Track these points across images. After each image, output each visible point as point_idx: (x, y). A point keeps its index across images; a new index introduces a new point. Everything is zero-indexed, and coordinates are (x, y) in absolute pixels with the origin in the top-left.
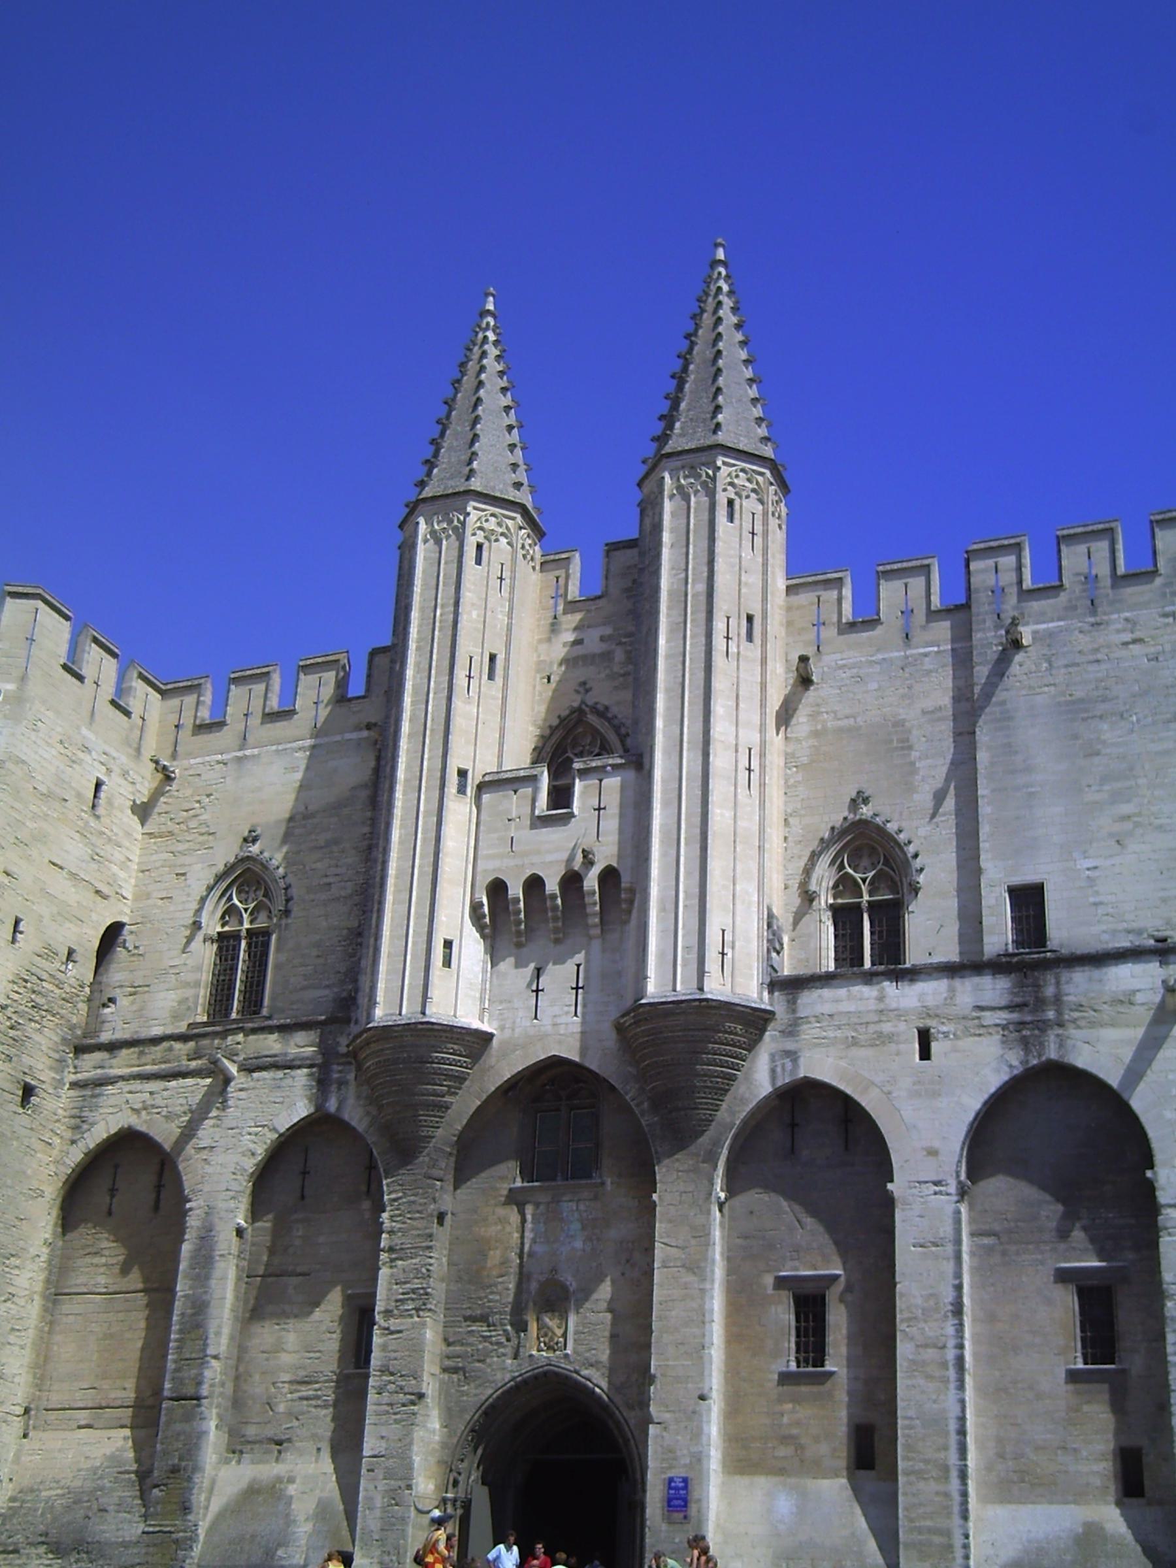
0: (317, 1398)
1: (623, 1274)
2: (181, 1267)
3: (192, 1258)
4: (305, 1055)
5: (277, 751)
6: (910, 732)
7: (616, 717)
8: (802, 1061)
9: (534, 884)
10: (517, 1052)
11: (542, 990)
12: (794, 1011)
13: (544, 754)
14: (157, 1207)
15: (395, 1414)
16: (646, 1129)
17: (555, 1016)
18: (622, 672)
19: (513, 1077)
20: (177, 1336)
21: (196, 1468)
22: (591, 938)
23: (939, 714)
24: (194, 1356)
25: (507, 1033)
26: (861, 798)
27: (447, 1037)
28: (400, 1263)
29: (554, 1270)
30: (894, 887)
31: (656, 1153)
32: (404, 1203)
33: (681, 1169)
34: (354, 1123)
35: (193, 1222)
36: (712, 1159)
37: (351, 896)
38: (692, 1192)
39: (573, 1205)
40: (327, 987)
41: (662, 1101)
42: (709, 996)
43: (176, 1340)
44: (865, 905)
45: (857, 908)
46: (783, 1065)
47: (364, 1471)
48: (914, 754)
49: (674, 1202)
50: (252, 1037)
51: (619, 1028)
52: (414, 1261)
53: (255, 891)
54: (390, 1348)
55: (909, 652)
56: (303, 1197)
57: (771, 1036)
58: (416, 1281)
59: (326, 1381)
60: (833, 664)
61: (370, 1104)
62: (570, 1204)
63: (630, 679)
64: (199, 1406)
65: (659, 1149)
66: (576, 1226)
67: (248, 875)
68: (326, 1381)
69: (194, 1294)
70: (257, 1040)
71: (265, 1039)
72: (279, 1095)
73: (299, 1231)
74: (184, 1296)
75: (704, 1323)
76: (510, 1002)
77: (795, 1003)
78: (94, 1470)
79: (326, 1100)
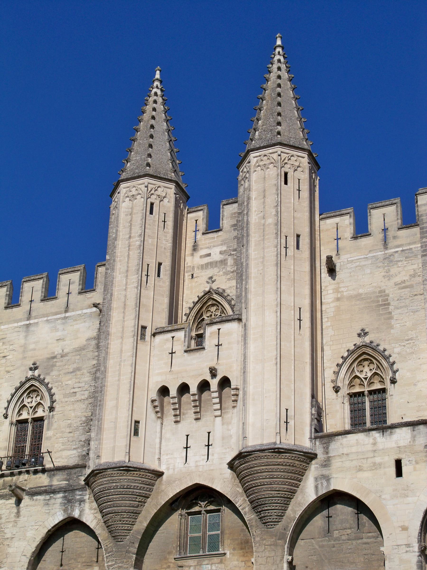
4: (62, 486)
5: (47, 320)
6: (388, 296)
7: (229, 295)
8: (332, 481)
10: (176, 482)
12: (327, 453)
18: (232, 270)
23: (404, 285)
25: (171, 472)
26: (363, 333)
27: (137, 474)
30: (382, 382)
32: (116, 567)
33: (267, 544)
34: (88, 523)
38: (273, 557)
39: (209, 566)
40: (74, 449)
42: (280, 446)
44: (366, 393)
45: (361, 394)
46: (322, 483)
48: (391, 308)
49: (263, 563)
51: (231, 465)
53: (36, 397)
55: (386, 252)
56: (61, 565)
57: (315, 467)
60: (346, 260)
61: (97, 513)
62: (208, 566)
65: (255, 533)
67: (32, 389)
70: (36, 478)
71: (40, 478)
72: (47, 509)
76: (172, 454)
77: (328, 448)
79: (73, 510)
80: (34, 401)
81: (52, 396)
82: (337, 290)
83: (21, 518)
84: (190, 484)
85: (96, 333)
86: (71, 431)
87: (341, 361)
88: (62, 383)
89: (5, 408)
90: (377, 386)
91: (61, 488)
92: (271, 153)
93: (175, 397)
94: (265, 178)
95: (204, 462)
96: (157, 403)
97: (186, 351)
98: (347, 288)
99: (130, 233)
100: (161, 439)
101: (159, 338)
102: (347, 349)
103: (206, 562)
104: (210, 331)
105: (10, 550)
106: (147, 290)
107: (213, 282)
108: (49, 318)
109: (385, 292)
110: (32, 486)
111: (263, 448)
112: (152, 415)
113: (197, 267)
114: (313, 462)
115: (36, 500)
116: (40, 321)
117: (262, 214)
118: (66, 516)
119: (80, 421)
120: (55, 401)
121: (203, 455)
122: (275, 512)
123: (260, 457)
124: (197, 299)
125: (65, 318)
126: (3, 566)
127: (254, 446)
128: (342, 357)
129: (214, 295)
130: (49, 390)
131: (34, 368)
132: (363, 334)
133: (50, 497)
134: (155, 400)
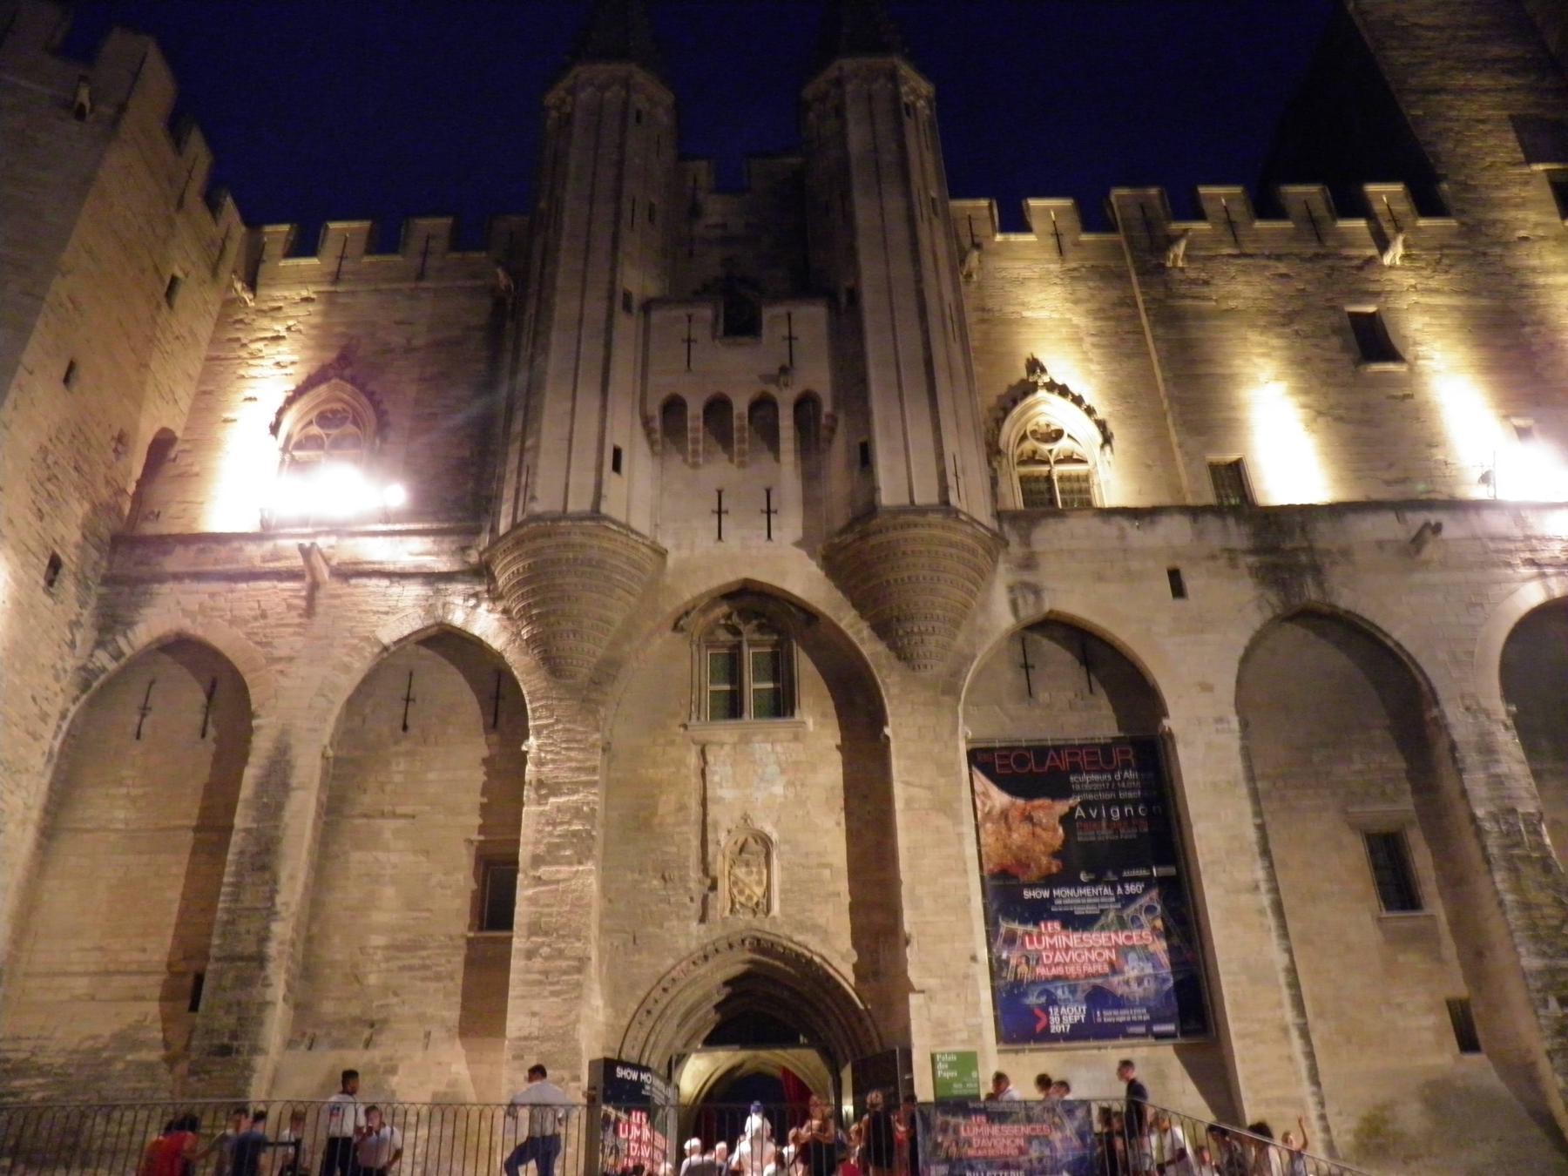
0: (425, 967)
15: (552, 984)
20: (231, 880)
21: (256, 1049)
25: (685, 553)
29: (745, 818)
35: (262, 745)
36: (951, 689)
43: (232, 884)
54: (542, 902)
56: (405, 728)
59: (440, 947)
64: (262, 967)
66: (773, 769)
68: (440, 947)
69: (257, 829)
73: (400, 765)
74: (248, 831)
75: (965, 871)
78: (97, 1051)
101: (656, 317)
103: (759, 737)
104: (771, 314)
105: (284, 682)
115: (356, 586)
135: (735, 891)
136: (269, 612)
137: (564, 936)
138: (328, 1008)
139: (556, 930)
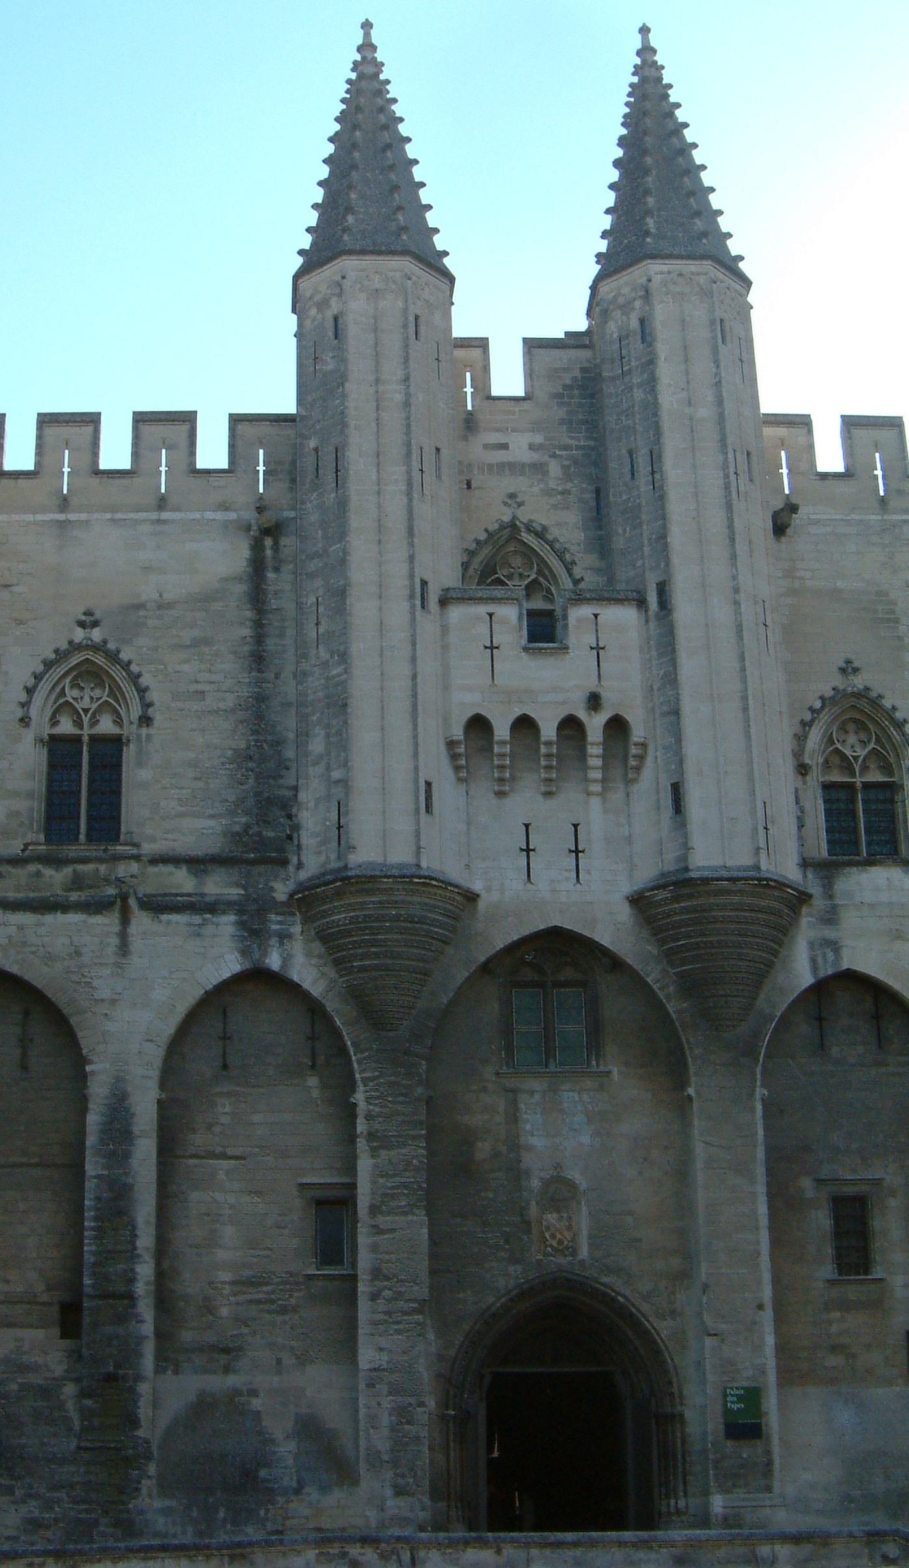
0: (273, 1302)
1: (640, 1173)
2: (88, 1143)
3: (102, 1131)
5: (112, 520)
8: (845, 953)
9: (525, 725)
11: (533, 850)
12: (831, 897)
13: (471, 571)
14: (25, 1067)
15: (398, 1323)
16: (674, 1016)
17: (553, 881)
18: (560, 489)
19: (506, 946)
21: (138, 1378)
22: (589, 794)
24: (119, 1247)
25: (495, 896)
26: (848, 669)
28: (383, 1153)
30: (887, 769)
31: (688, 1042)
34: (306, 985)
35: (99, 1090)
36: (750, 1051)
37: (233, 711)
40: (212, 817)
41: (690, 986)
43: (92, 1229)
44: (859, 785)
45: (850, 787)
46: (824, 955)
47: (362, 1386)
50: (152, 870)
51: (637, 901)
52: (403, 1151)
53: (92, 688)
55: (885, 517)
56: (225, 1067)
58: (407, 1174)
59: (282, 1283)
61: (325, 965)
62: (572, 1094)
63: (572, 498)
64: (134, 1306)
65: (691, 1040)
67: (83, 668)
68: (282, 1283)
69: (108, 1176)
71: (171, 874)
73: (225, 1107)
74: (95, 1177)
79: (265, 954)
80: (87, 698)
81: (142, 691)
82: (790, 574)
83: (136, 961)
84: (542, 927)
85: (243, 569)
86: (199, 775)
87: (808, 716)
88: (166, 667)
89: (23, 705)
90: (875, 776)
91: (230, 904)
92: (693, 273)
93: (503, 743)
94: (683, 321)
95: (570, 885)
96: (461, 749)
97: (525, 649)
98: (811, 574)
99: (377, 369)
100: (469, 824)
101: (456, 613)
102: (820, 694)
105: (111, 1027)
106: (423, 501)
107: (519, 506)
108: (119, 516)
109: (887, 594)
110: (149, 890)
111: (735, 874)
112: (449, 773)
113: (479, 468)
114: (804, 910)
115: (169, 923)
116: (97, 519)
117: (684, 395)
118: (248, 965)
119: (219, 757)
120: (150, 705)
121: (566, 870)
122: (739, 1002)
123: (729, 892)
124: (483, 536)
125: (159, 521)
126: (95, 1059)
127: (714, 869)
128: (810, 709)
129: (523, 534)
130: (135, 678)
131: (89, 622)
132: (850, 670)
133: (204, 920)
134: (459, 742)
135: (547, 1235)
136: (84, 950)
137: (402, 1281)
138: (187, 1336)
139: (395, 1276)
